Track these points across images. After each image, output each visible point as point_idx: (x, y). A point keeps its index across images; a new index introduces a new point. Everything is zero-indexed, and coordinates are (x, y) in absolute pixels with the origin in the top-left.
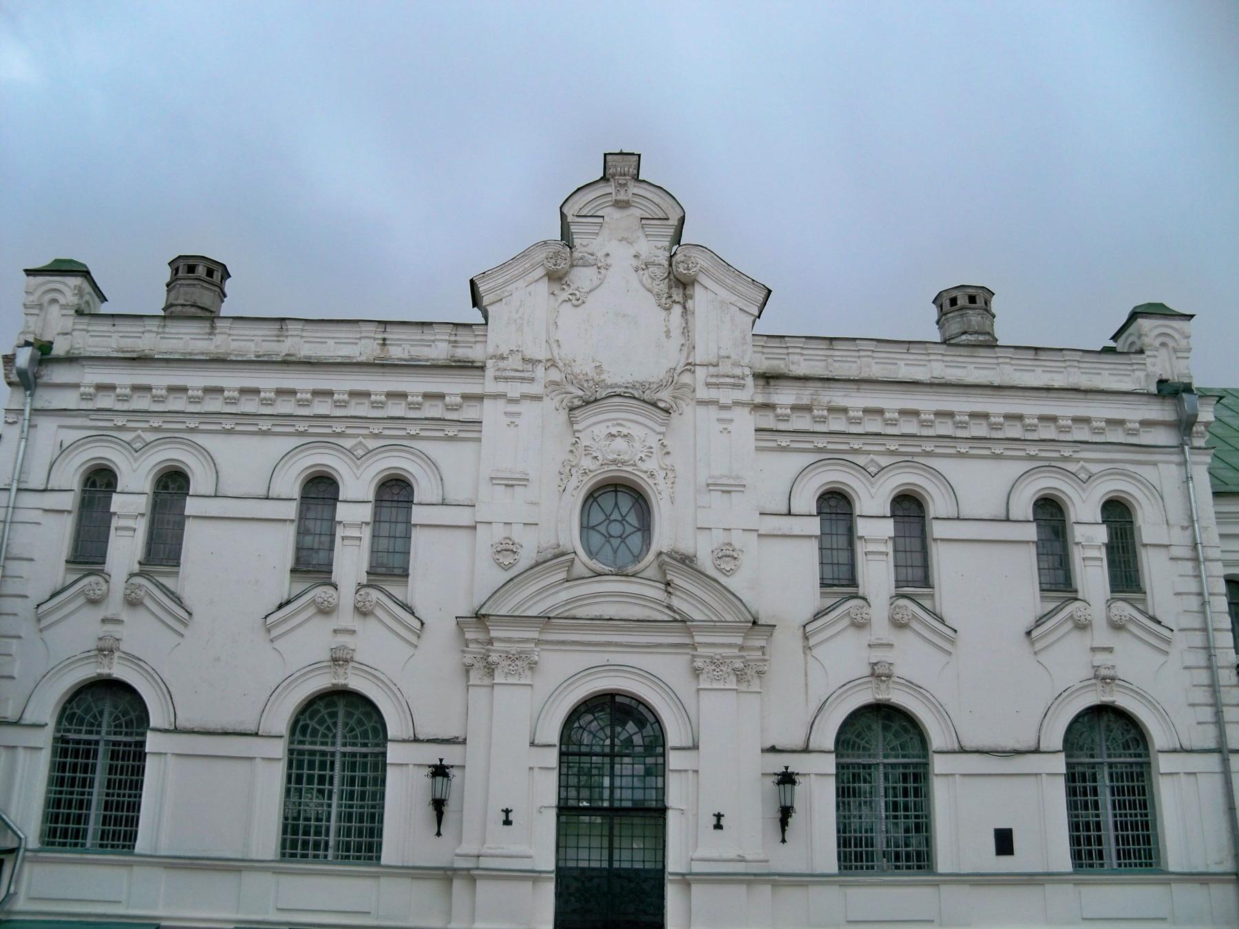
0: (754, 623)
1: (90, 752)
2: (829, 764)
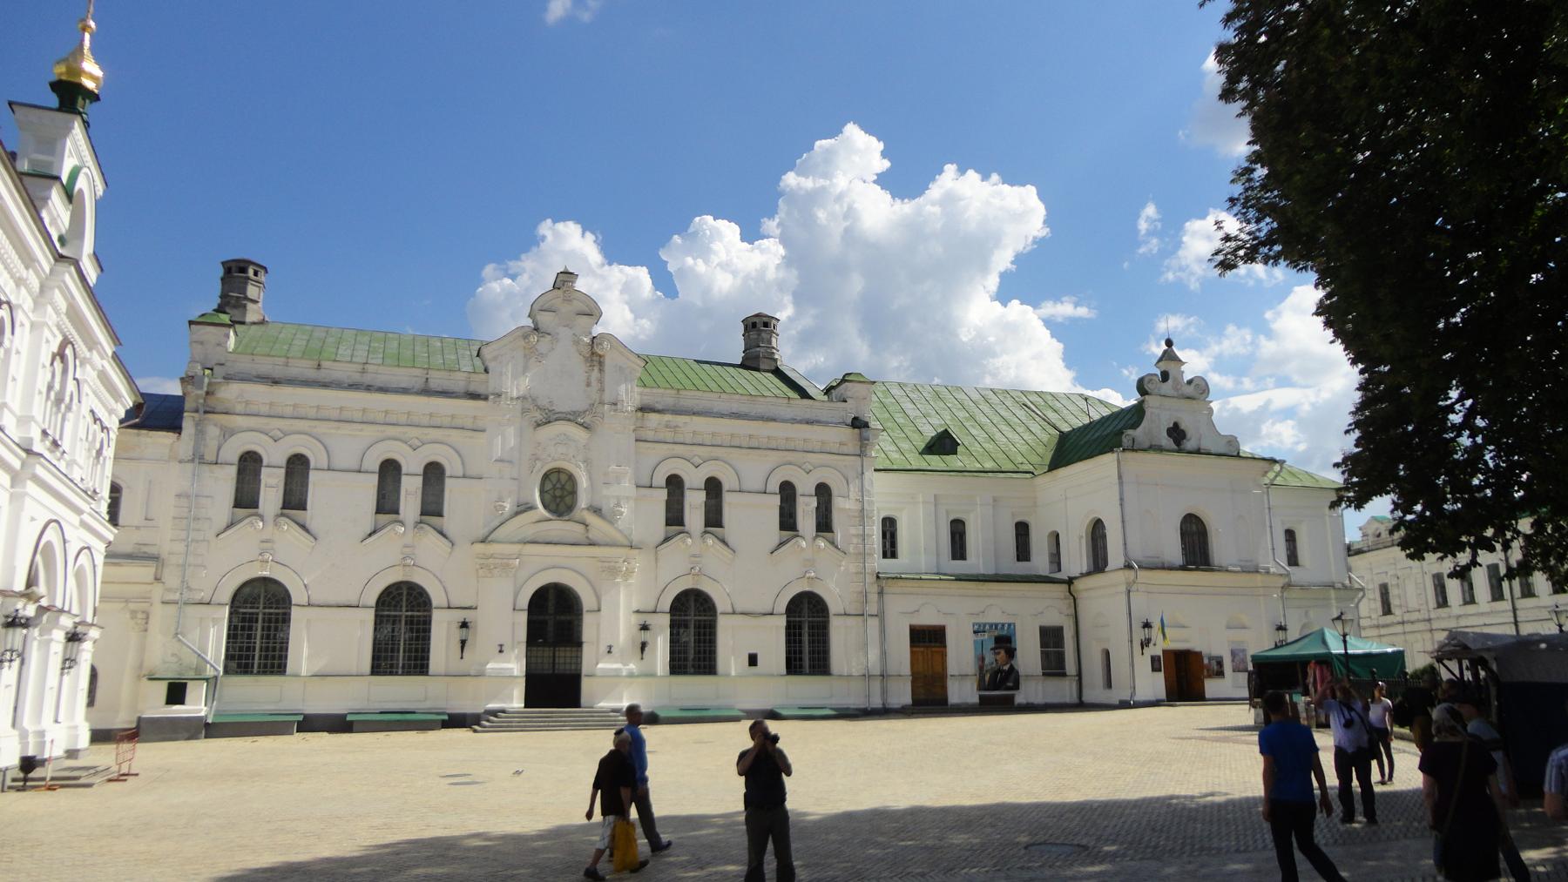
1: (252, 619)
2: (665, 620)
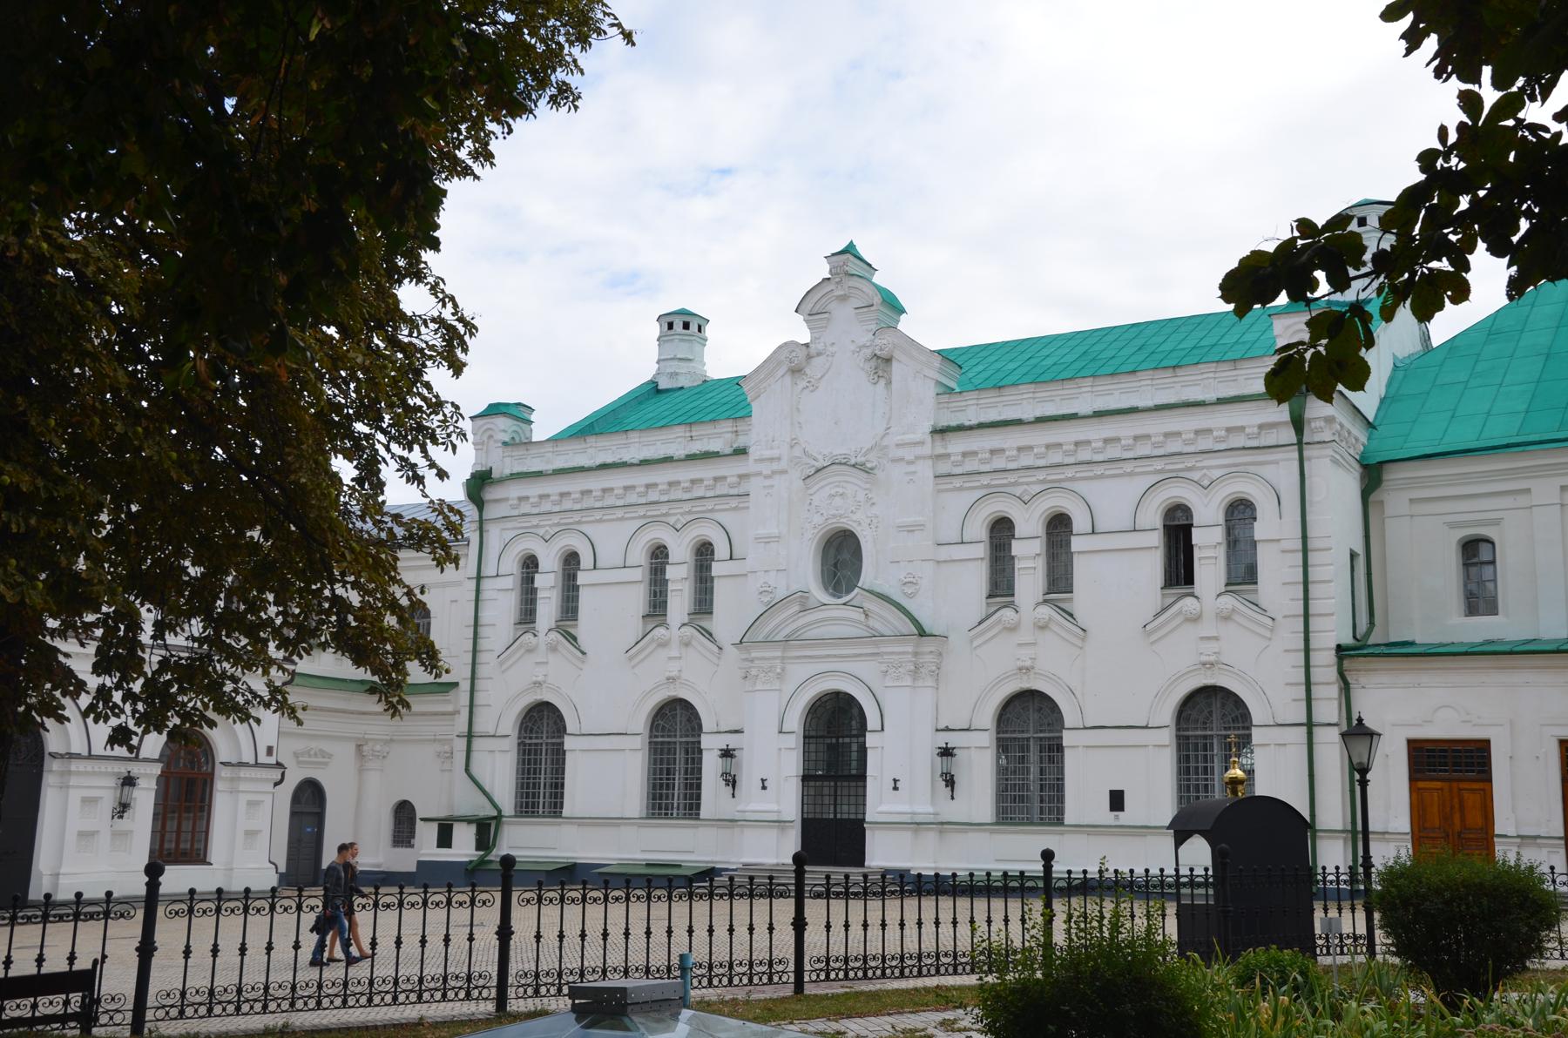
0: (922, 633)
2: (987, 739)
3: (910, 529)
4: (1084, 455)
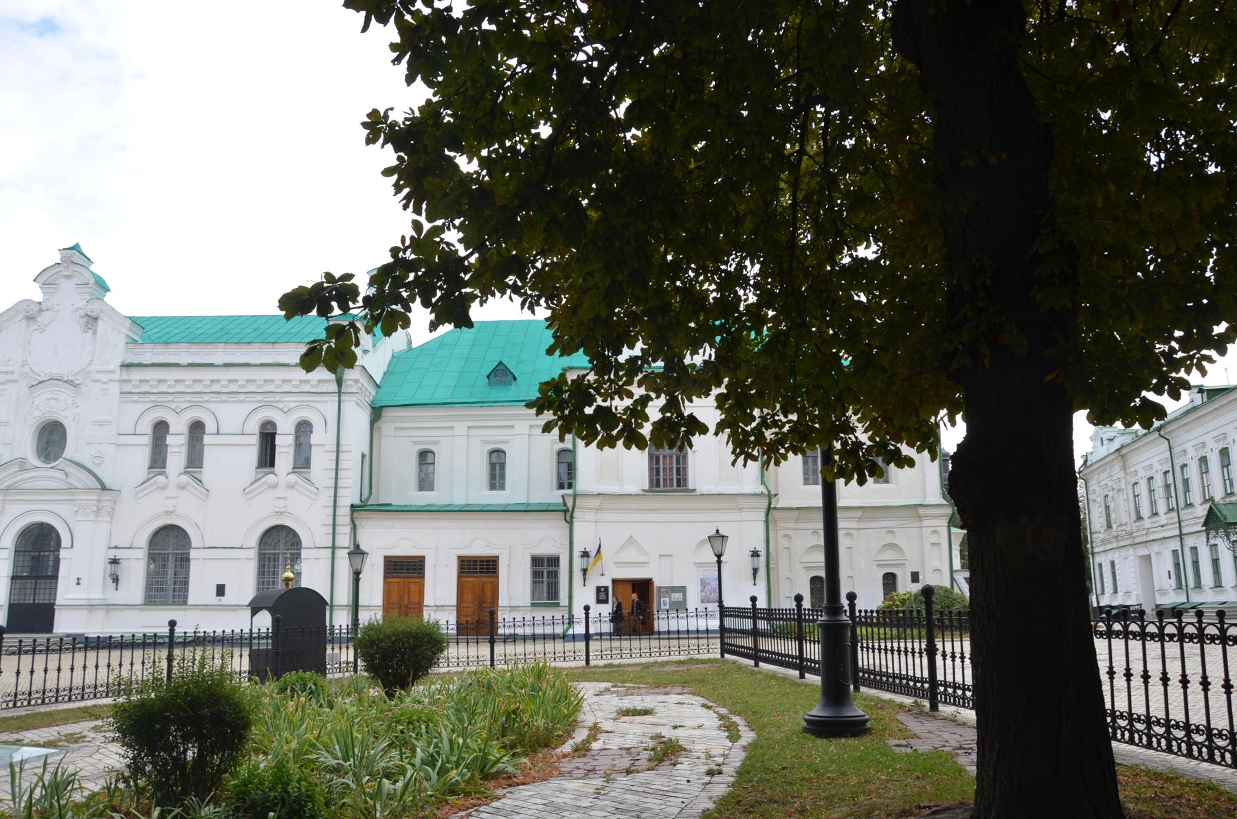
0: (104, 488)
2: (142, 554)
3: (101, 424)
4: (216, 388)
